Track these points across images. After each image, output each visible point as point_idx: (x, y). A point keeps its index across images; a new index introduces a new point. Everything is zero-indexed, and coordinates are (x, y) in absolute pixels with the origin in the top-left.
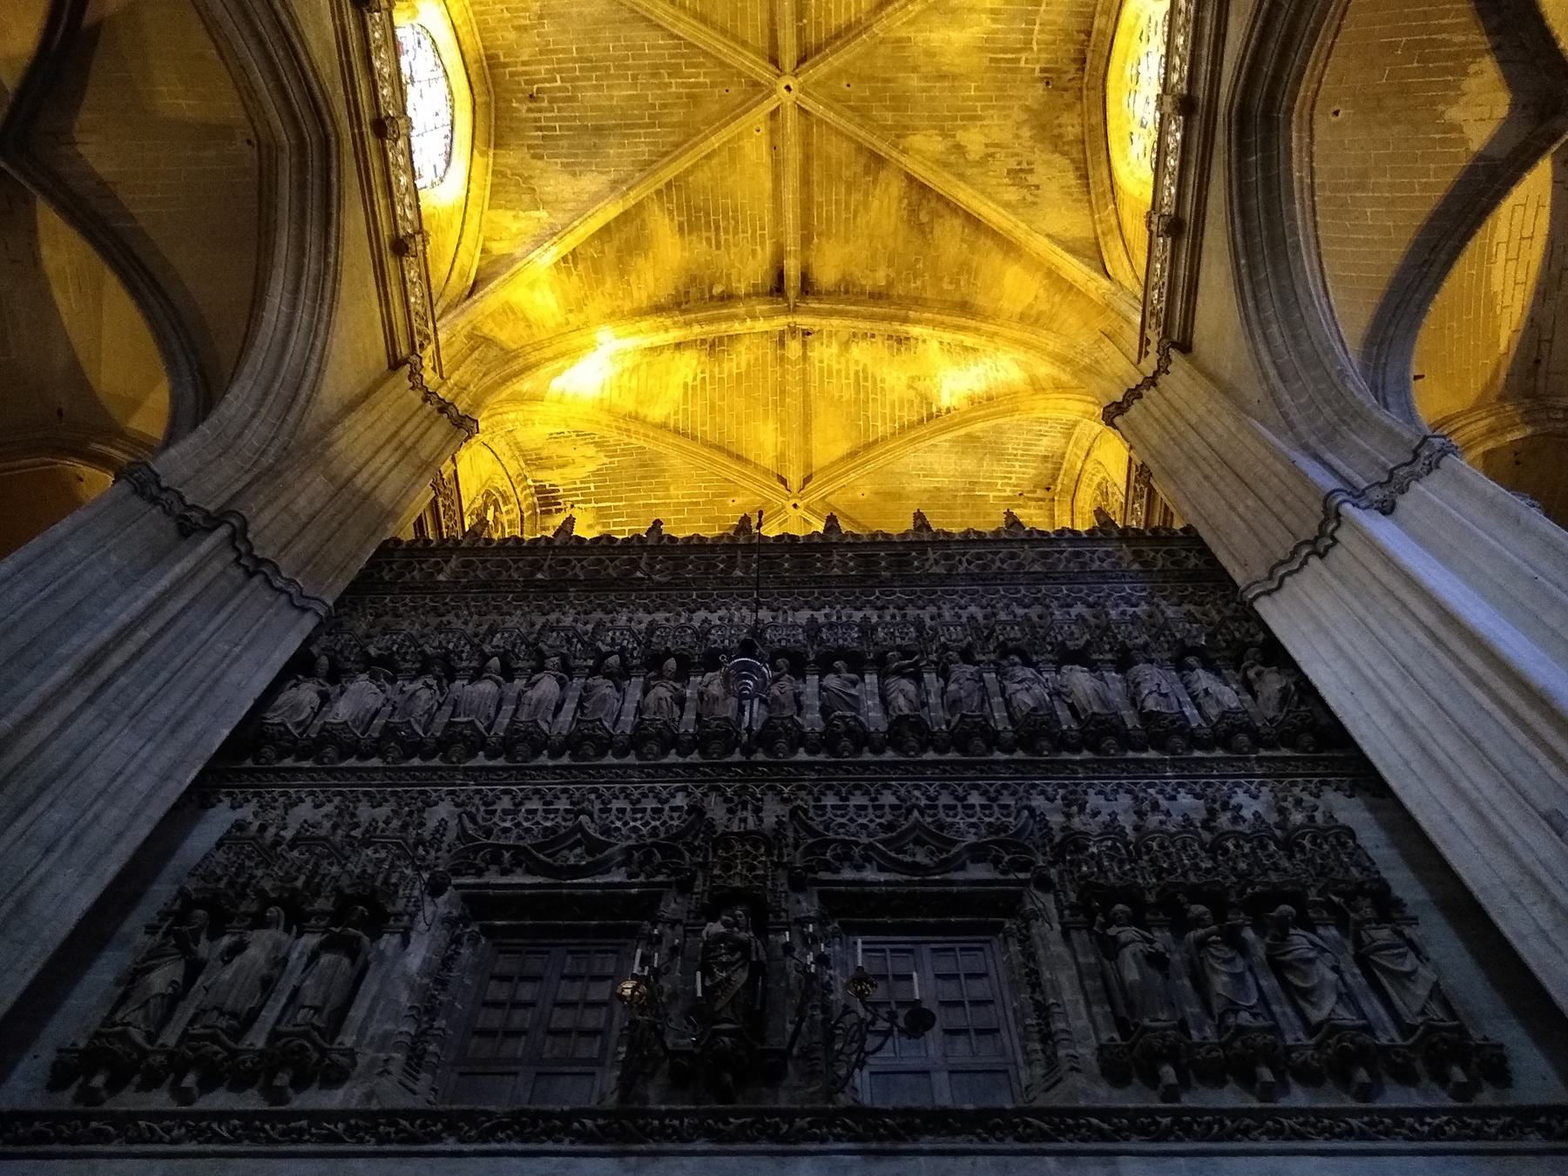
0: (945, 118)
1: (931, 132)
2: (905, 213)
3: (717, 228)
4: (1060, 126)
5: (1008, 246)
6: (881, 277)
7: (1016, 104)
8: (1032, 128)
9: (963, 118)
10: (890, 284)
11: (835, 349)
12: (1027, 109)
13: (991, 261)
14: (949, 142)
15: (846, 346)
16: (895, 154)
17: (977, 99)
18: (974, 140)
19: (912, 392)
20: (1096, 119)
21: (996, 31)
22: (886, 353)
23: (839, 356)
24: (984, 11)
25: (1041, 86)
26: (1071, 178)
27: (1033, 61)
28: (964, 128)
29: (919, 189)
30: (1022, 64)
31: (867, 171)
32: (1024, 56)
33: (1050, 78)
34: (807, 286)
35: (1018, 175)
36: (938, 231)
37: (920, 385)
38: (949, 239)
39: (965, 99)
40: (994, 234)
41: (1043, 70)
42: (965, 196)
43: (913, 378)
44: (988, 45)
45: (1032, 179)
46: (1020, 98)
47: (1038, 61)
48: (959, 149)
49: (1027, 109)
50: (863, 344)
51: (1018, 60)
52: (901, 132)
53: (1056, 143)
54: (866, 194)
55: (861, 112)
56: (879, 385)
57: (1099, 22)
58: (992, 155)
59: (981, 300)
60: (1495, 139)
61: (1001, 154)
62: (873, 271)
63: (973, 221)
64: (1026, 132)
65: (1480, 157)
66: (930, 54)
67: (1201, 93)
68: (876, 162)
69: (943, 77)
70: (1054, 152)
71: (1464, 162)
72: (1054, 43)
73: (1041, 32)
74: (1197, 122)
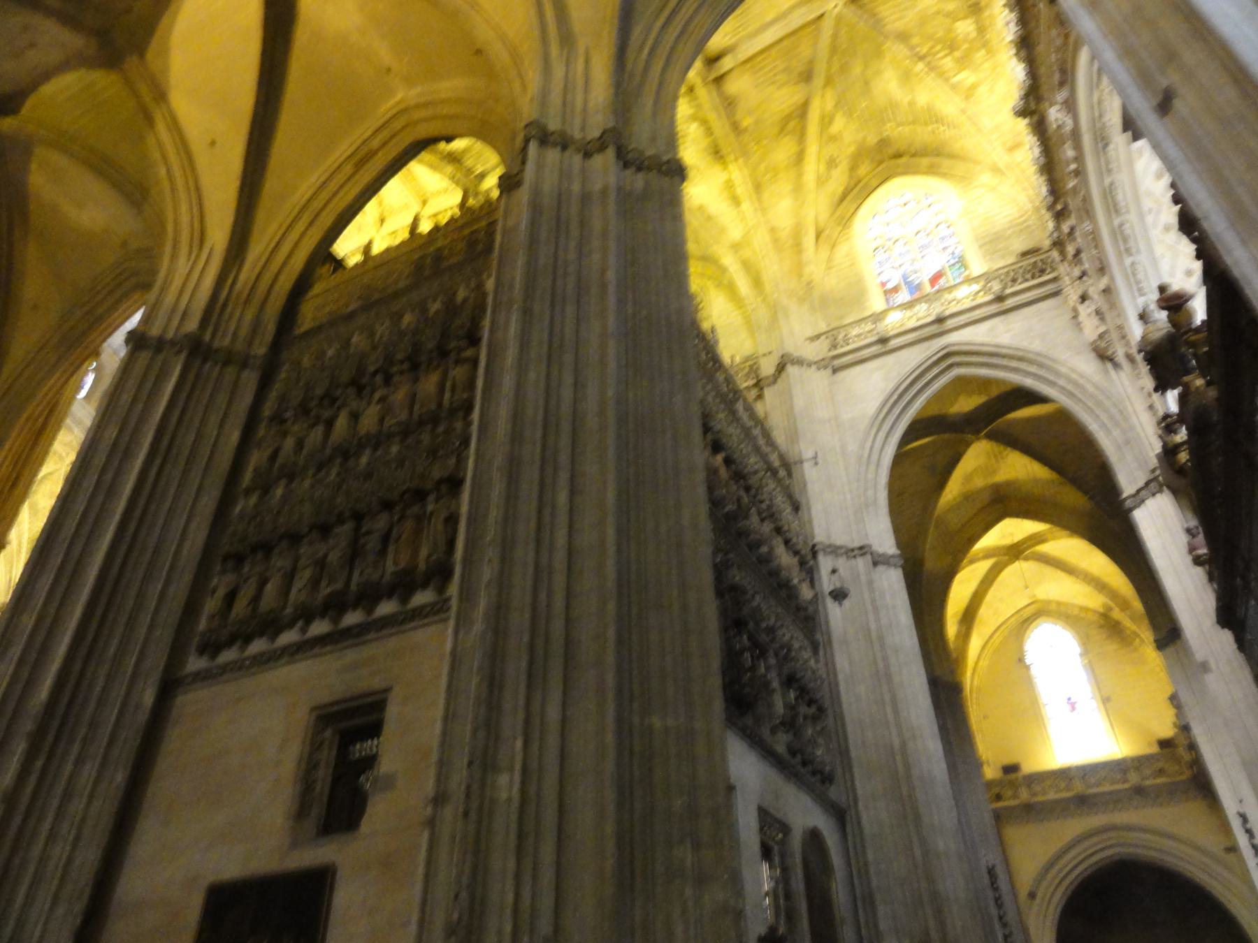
5: (798, 188)
6: (747, 122)
10: (746, 130)
13: (784, 186)
15: (694, 118)
18: (839, 124)
20: (875, 183)
27: (890, 130)
29: (802, 111)
33: (883, 143)
34: (719, 80)
35: (831, 163)
36: (786, 139)
38: (783, 151)
40: (800, 175)
42: (812, 149)
44: (893, 105)
50: (702, 129)
52: (829, 82)
53: (853, 168)
55: (834, 49)
57: (925, 161)
63: (800, 157)
64: (852, 149)
67: (950, 323)
68: (807, 76)
71: (944, 411)
74: (934, 329)
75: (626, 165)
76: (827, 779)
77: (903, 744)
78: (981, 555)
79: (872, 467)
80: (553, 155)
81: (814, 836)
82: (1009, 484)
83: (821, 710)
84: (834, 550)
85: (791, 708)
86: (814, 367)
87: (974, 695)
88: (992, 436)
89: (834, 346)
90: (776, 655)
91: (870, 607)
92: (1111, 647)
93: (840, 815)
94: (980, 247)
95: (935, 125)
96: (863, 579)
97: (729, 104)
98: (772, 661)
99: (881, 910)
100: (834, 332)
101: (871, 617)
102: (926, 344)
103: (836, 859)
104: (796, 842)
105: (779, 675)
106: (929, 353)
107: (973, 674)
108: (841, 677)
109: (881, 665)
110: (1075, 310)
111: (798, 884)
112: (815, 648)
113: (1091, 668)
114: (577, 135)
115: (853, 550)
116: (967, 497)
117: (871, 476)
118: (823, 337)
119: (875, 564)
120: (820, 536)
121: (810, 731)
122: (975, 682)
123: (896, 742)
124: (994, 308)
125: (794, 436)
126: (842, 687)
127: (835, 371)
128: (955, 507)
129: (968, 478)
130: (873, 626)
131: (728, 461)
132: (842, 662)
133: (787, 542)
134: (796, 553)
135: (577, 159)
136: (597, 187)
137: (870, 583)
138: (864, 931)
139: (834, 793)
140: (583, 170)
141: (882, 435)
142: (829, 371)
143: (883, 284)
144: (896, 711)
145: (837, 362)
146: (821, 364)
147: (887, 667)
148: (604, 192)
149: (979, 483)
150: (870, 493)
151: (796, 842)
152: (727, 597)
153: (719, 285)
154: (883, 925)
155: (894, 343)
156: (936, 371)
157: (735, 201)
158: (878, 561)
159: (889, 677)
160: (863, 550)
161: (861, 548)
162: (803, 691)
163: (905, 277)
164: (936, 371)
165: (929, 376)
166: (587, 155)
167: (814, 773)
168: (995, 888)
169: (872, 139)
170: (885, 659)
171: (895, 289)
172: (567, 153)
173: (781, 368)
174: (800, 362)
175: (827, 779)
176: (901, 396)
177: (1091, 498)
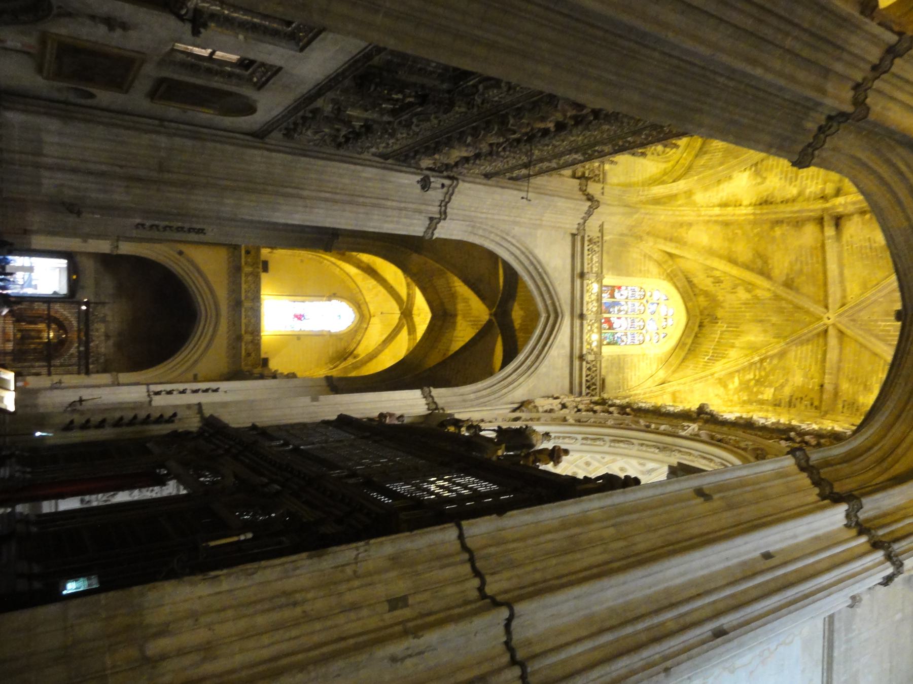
0: (757, 303)
1: (763, 298)
2: (770, 261)
3: (871, 248)
4: (707, 301)
5: (711, 252)
6: (778, 231)
7: (727, 309)
8: (718, 300)
9: (749, 304)
11: (808, 191)
12: (722, 307)
13: (718, 244)
14: (754, 293)
15: (800, 194)
16: (773, 288)
17: (745, 312)
18: (743, 295)
19: (764, 175)
20: (690, 304)
21: (734, 339)
22: (776, 193)
23: (805, 188)
24: (738, 347)
25: (719, 317)
26: (695, 281)
27: (721, 327)
28: (749, 300)
29: (765, 273)
30: (725, 326)
31: (792, 280)
32: (724, 329)
33: (715, 320)
34: (820, 221)
35: (718, 281)
37: (759, 180)
38: (743, 251)
39: (749, 312)
40: (721, 257)
41: (717, 323)
42: (735, 271)
43: (762, 183)
44: (738, 334)
45: (711, 279)
46: (726, 312)
47: (719, 327)
48: (749, 291)
49: (722, 307)
50: (789, 196)
51: (727, 327)
52: (777, 297)
53: (706, 294)
54: (792, 269)
55: (798, 308)
56: (783, 176)
57: (690, 341)
58: (733, 289)
59: (717, 228)
60: (512, 306)
61: (729, 289)
62: (783, 234)
63: (733, 261)
64: (721, 298)
65: (514, 300)
66: (765, 331)
67: (577, 322)
68: (788, 284)
69: (761, 321)
70: (706, 291)
71: (517, 298)
72: (711, 334)
73: (715, 338)
74: (577, 311)
75: (830, 118)
76: (289, 134)
77: (301, 197)
78: (411, 292)
79: (498, 239)
80: (874, 54)
81: (250, 109)
82: (454, 323)
83: (339, 146)
84: (449, 195)
85: (348, 122)
86: (581, 221)
87: (318, 258)
88: (489, 324)
89: (590, 241)
90: (389, 123)
91: (403, 205)
92: (331, 351)
93: (260, 135)
94: (618, 356)
95: (710, 354)
96: (423, 207)
97: (798, 223)
98: (386, 118)
99: (189, 143)
100: (600, 244)
101: (395, 204)
102: (569, 301)
103: (228, 121)
104: (247, 92)
105: (374, 121)
106: (562, 301)
107: (334, 264)
108: (359, 168)
109: (361, 200)
110: (557, 398)
111: (217, 83)
112: (385, 157)
113: (320, 335)
114: (877, 84)
115: (446, 206)
116: (453, 296)
117: (492, 236)
118: (600, 235)
119: (431, 219)
120: (462, 186)
121: (327, 130)
122: (325, 261)
123: (306, 193)
124: (577, 352)
125: (541, 192)
126: (352, 167)
127: (573, 235)
128: (449, 287)
129: (466, 300)
130: (389, 203)
131: (546, 132)
132: (370, 172)
133: (466, 160)
134: (456, 164)
135: (859, 77)
136: (830, 87)
137: (420, 212)
138: (173, 124)
139: (277, 136)
140: (848, 78)
141: (518, 253)
142: (575, 231)
143: (619, 288)
144: (326, 200)
145: (579, 238)
146: (582, 227)
147: (358, 204)
148: (824, 92)
149: (460, 306)
150: (481, 232)
151: (247, 92)
152: (447, 95)
153: (665, 173)
154: (178, 141)
155: (578, 282)
156: (549, 302)
157: (724, 205)
158: (433, 222)
159: (350, 203)
160: (443, 215)
161: (445, 213)
162: (357, 135)
163: (617, 304)
164: (549, 302)
165: (547, 297)
166: (857, 87)
167: (295, 124)
168: (190, 230)
169: (720, 313)
170: (364, 205)
171: (612, 296)
172: (868, 67)
173: (590, 198)
174: (589, 213)
175: (289, 134)
176: (540, 274)
177: (430, 369)
